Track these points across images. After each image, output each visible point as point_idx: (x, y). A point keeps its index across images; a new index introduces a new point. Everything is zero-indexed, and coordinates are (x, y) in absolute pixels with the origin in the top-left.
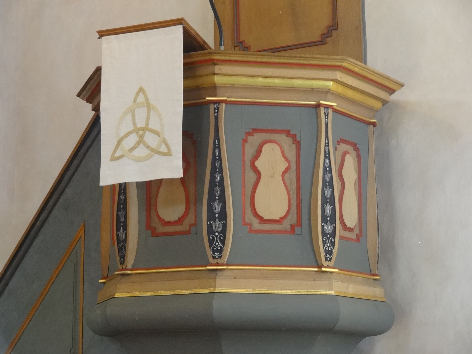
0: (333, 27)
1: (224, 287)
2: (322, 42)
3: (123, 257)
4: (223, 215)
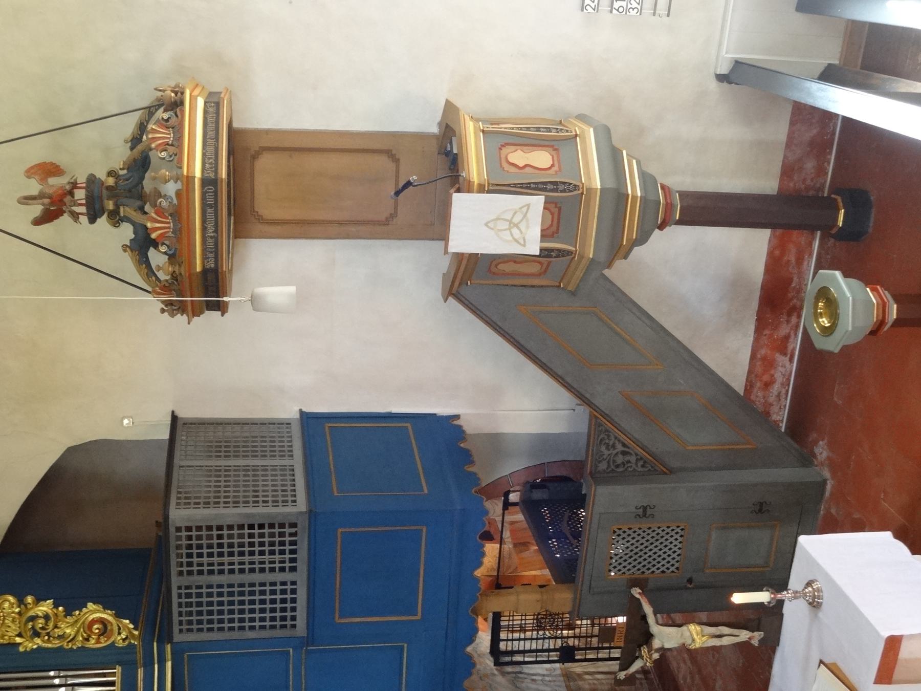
0: (389, 154)
1: (598, 185)
2: (396, 161)
3: (569, 253)
4: (555, 183)
